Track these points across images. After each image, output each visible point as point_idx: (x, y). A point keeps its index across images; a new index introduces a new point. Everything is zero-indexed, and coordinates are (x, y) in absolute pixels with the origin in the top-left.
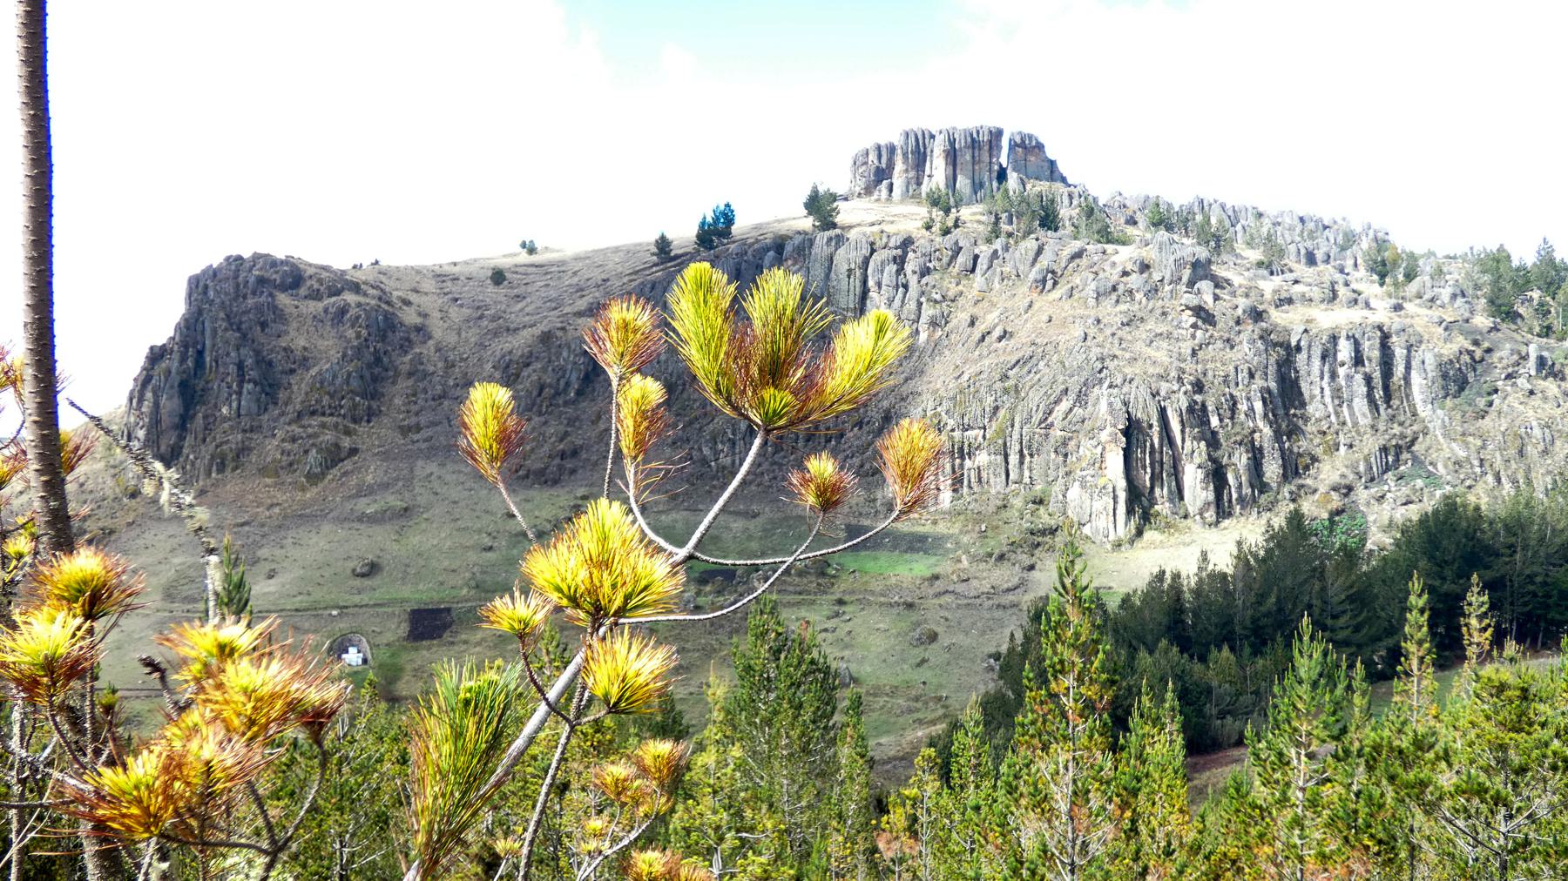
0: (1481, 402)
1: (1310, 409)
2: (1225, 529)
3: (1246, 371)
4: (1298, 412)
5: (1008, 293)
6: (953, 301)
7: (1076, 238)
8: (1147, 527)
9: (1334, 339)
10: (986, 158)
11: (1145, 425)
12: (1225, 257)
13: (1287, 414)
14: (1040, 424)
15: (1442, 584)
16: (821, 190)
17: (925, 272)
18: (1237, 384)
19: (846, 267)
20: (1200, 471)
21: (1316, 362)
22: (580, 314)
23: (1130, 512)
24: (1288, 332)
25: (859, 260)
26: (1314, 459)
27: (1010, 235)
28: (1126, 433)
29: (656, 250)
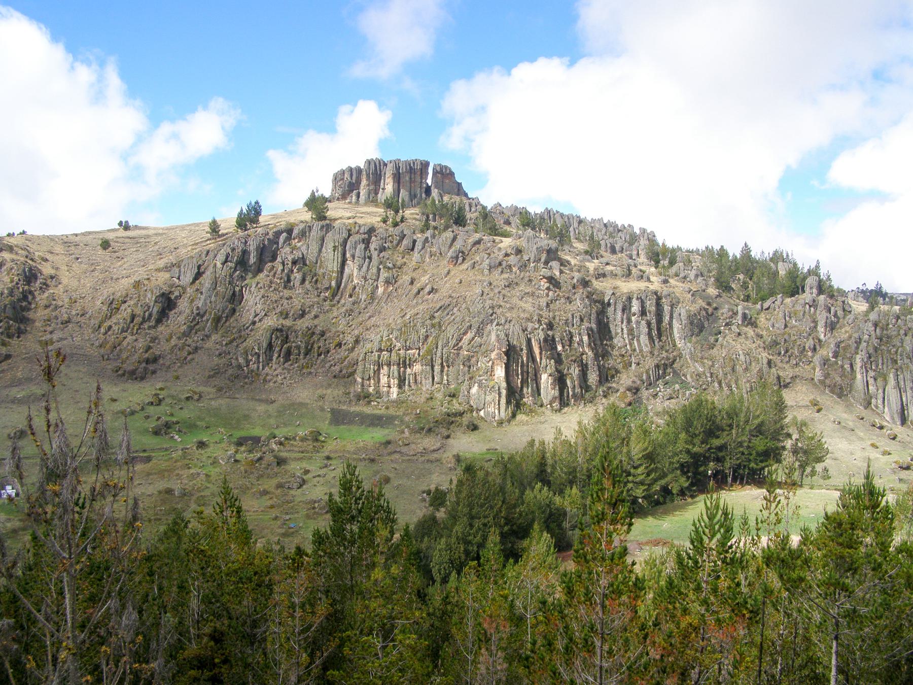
0: (712, 339)
1: (615, 341)
2: (565, 413)
3: (578, 317)
4: (608, 343)
5: (435, 265)
6: (400, 268)
7: (476, 232)
8: (519, 412)
9: (630, 299)
10: (418, 179)
11: (518, 349)
12: (566, 247)
13: (602, 344)
14: (454, 347)
15: (693, 447)
16: (316, 194)
17: (382, 249)
18: (573, 325)
19: (333, 245)
20: (550, 378)
21: (619, 313)
22: (158, 270)
23: (508, 402)
24: (603, 294)
25: (341, 240)
26: (617, 372)
27: (435, 228)
28: (507, 353)
29: (209, 230)
